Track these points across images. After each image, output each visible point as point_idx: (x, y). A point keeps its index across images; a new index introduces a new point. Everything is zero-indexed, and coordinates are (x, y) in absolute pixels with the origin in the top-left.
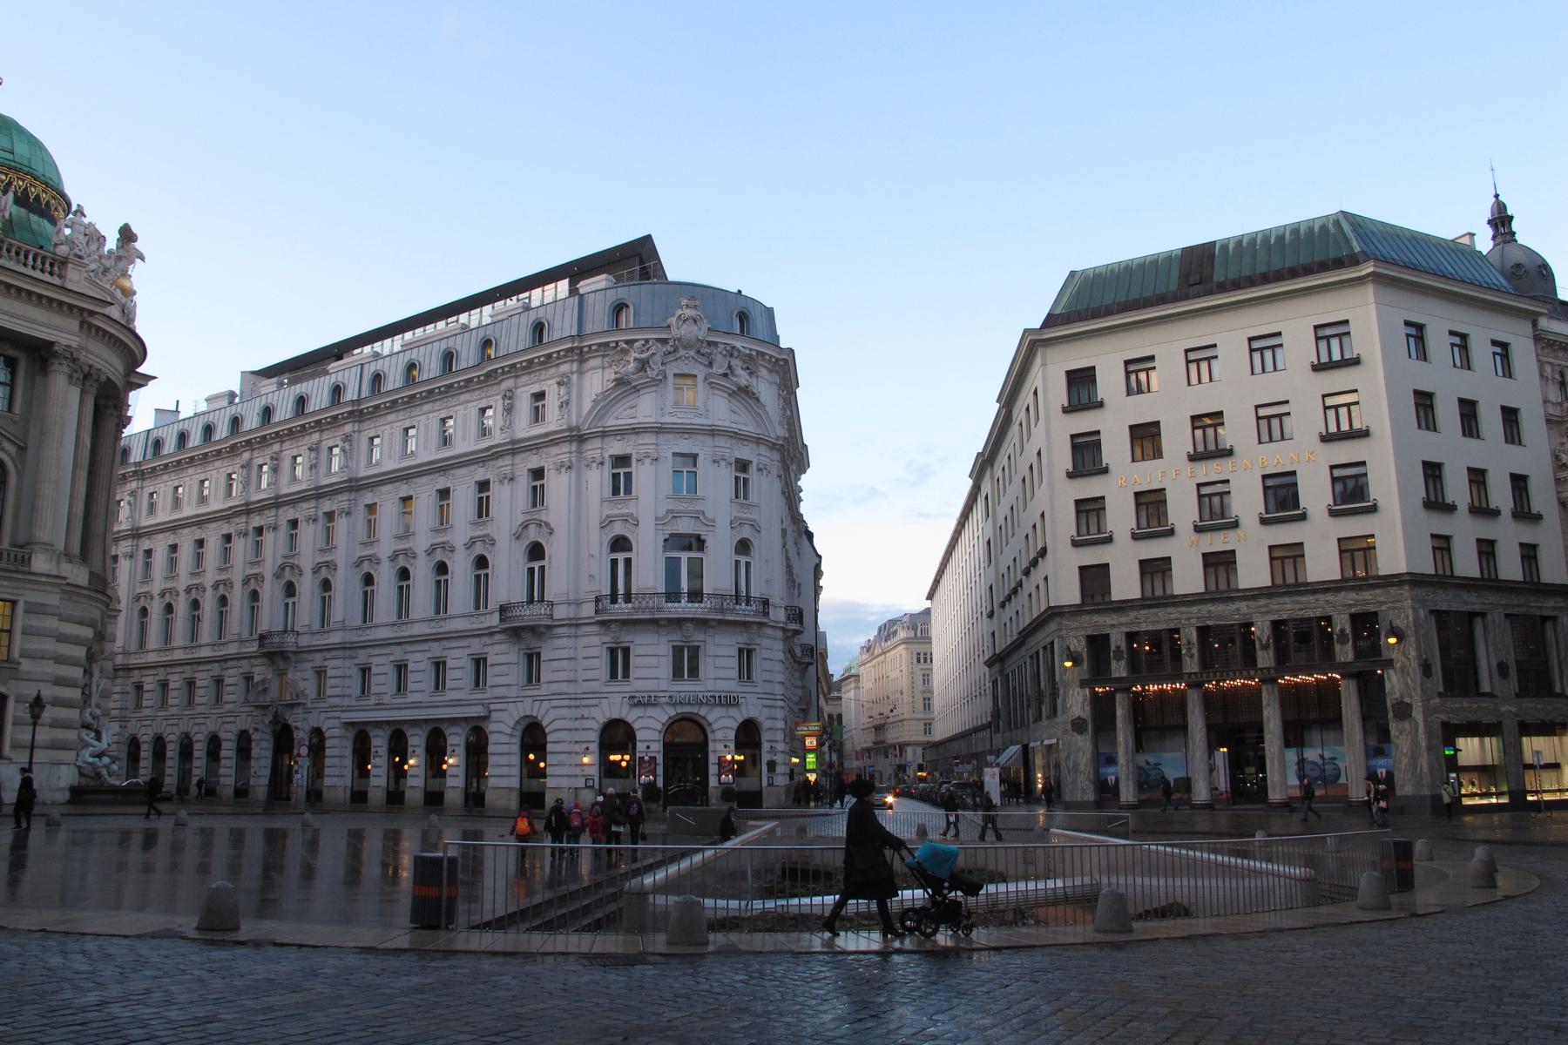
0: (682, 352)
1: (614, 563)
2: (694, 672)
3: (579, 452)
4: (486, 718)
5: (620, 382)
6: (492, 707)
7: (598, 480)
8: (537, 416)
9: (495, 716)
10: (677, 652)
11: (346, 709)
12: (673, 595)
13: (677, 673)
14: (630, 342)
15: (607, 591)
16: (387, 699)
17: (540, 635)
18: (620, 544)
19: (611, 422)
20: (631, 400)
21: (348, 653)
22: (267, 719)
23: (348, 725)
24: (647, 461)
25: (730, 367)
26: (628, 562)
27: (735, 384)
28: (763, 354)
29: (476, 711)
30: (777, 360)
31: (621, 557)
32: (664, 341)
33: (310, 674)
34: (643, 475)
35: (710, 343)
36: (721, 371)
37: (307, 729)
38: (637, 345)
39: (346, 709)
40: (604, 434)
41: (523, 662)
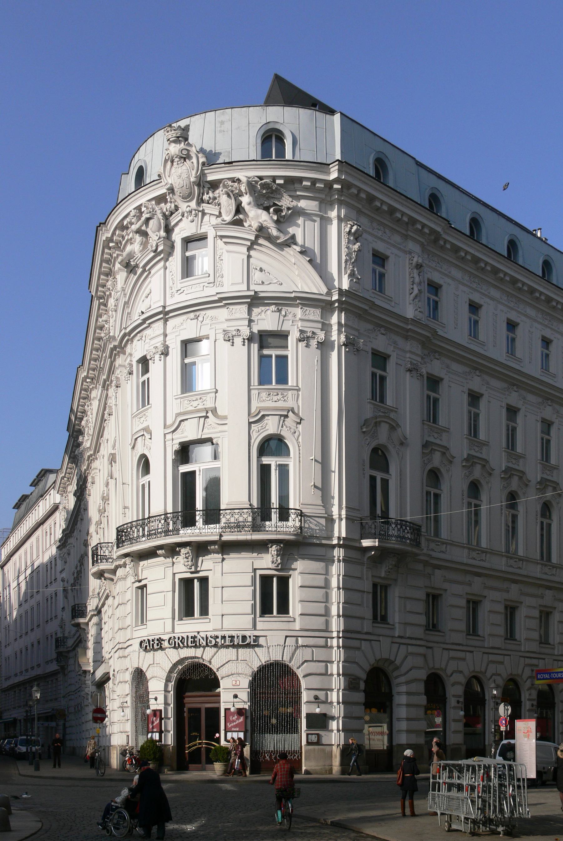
0: (183, 207)
10: (187, 584)
13: (187, 611)
25: (239, 209)
28: (300, 180)
35: (214, 185)
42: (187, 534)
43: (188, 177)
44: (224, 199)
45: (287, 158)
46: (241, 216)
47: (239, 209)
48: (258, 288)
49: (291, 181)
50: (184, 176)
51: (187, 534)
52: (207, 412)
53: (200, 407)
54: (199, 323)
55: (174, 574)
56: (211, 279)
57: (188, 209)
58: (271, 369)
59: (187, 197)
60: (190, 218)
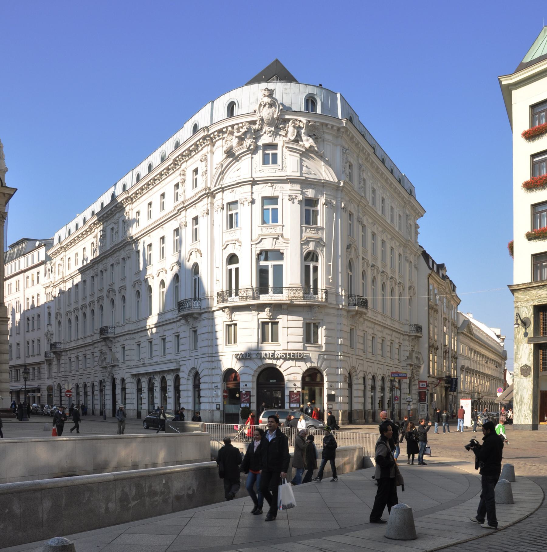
1: (230, 270)
2: (275, 339)
3: (212, 204)
4: (178, 370)
5: (230, 153)
6: (181, 363)
7: (220, 218)
8: (195, 183)
9: (182, 368)
11: (134, 367)
12: (263, 288)
14: (232, 126)
15: (225, 288)
16: (146, 361)
17: (196, 319)
18: (233, 259)
19: (228, 180)
20: (237, 165)
21: (132, 336)
22: (107, 374)
23: (134, 375)
24: (246, 203)
25: (299, 135)
26: (237, 269)
27: (303, 146)
28: (327, 125)
29: (173, 366)
30: (339, 129)
31: (233, 267)
32: (254, 123)
33: (120, 349)
34: (243, 212)
36: (292, 138)
37: (120, 379)
38: (236, 127)
39: (134, 367)
40: (223, 189)
41: (192, 334)
42: (264, 299)
43: (273, 115)
44: (291, 129)
45: (318, 113)
46: (299, 139)
47: (299, 135)
48: (307, 176)
49: (322, 124)
50: (271, 114)
51: (264, 299)
52: (279, 236)
53: (274, 232)
54: (273, 189)
55: (258, 319)
56: (280, 167)
57: (269, 130)
58: (308, 217)
59: (269, 125)
60: (269, 135)
